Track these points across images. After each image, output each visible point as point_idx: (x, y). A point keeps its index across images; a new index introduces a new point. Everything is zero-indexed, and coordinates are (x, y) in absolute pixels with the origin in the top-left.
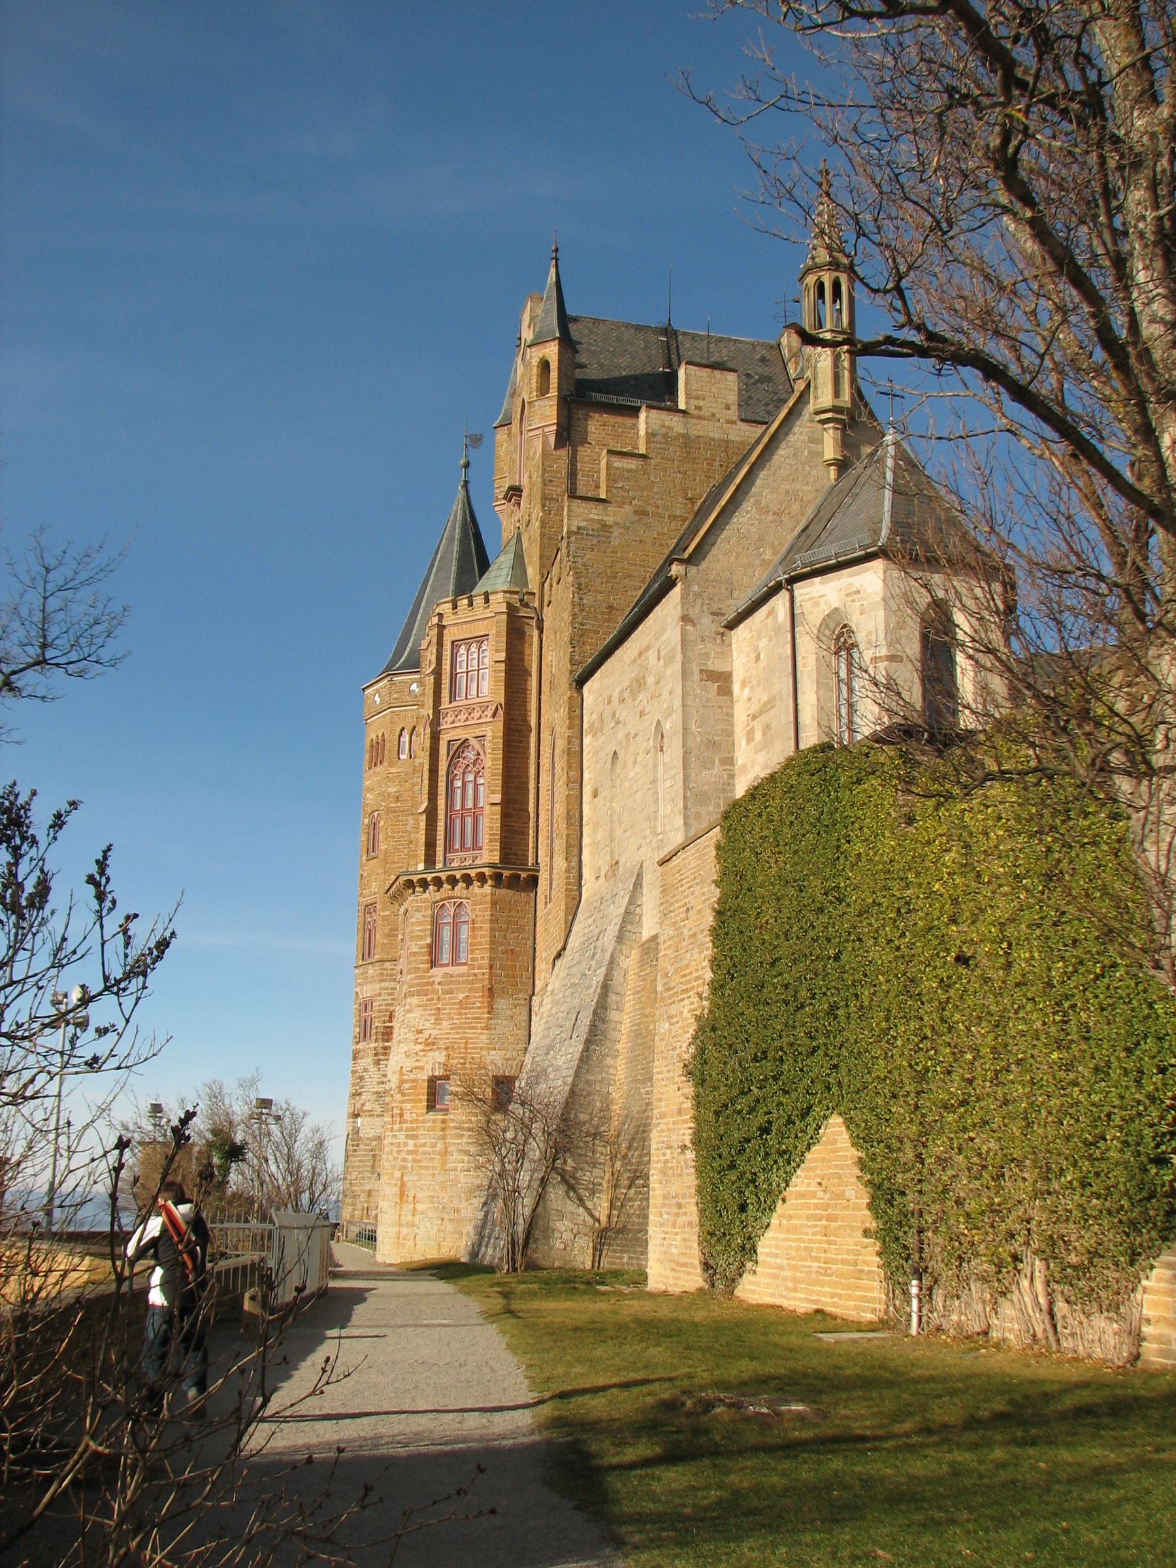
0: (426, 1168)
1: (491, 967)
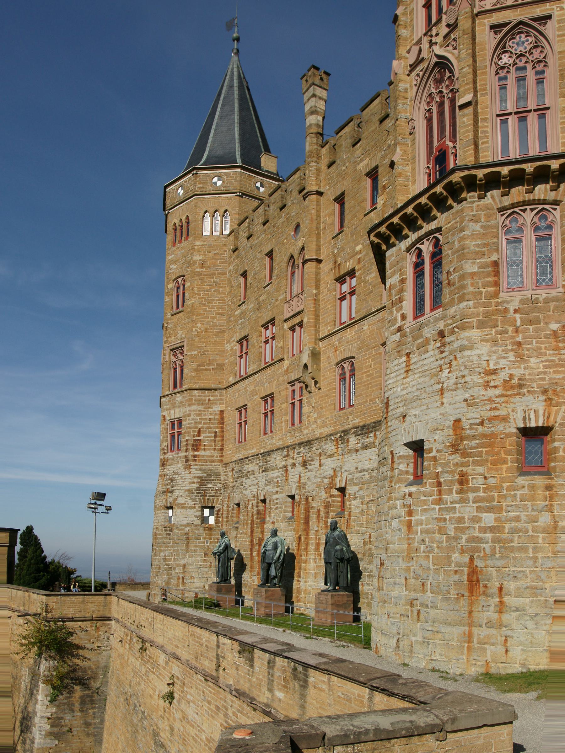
0: (524, 549)
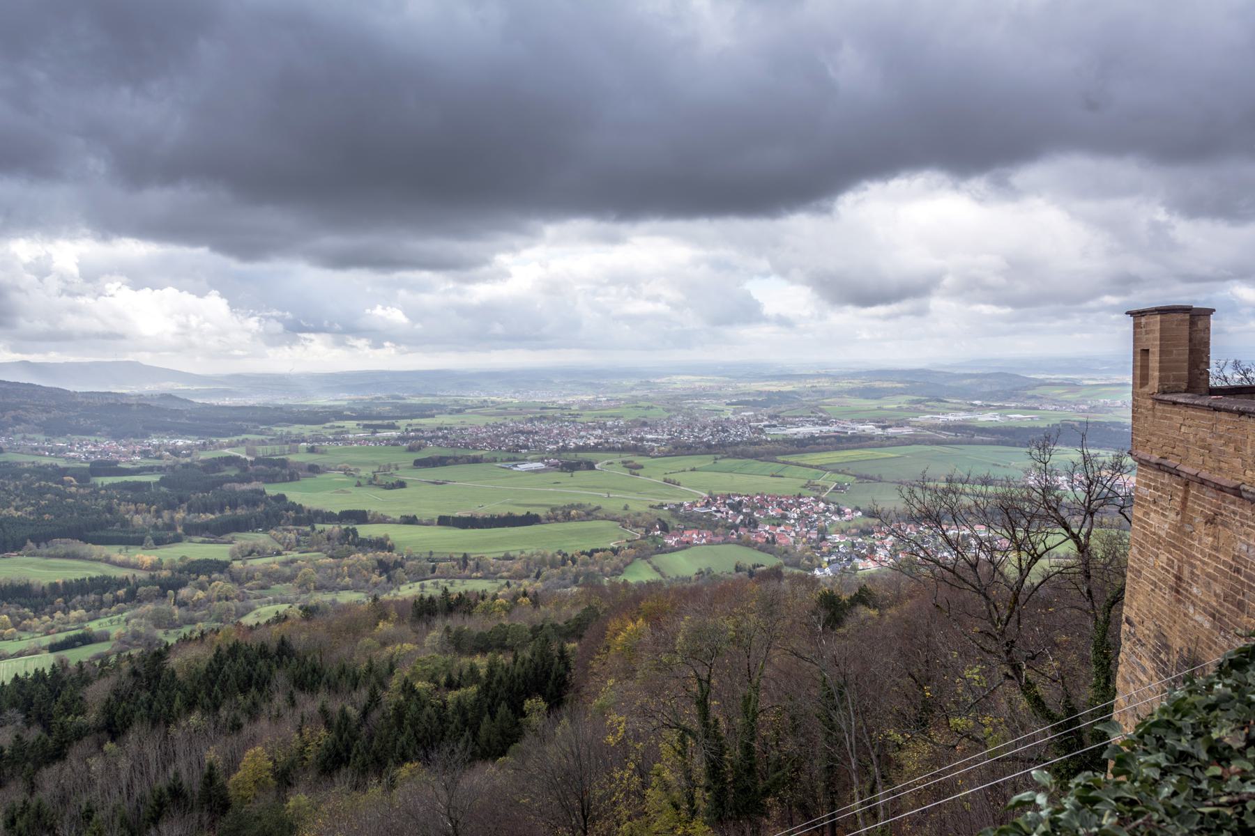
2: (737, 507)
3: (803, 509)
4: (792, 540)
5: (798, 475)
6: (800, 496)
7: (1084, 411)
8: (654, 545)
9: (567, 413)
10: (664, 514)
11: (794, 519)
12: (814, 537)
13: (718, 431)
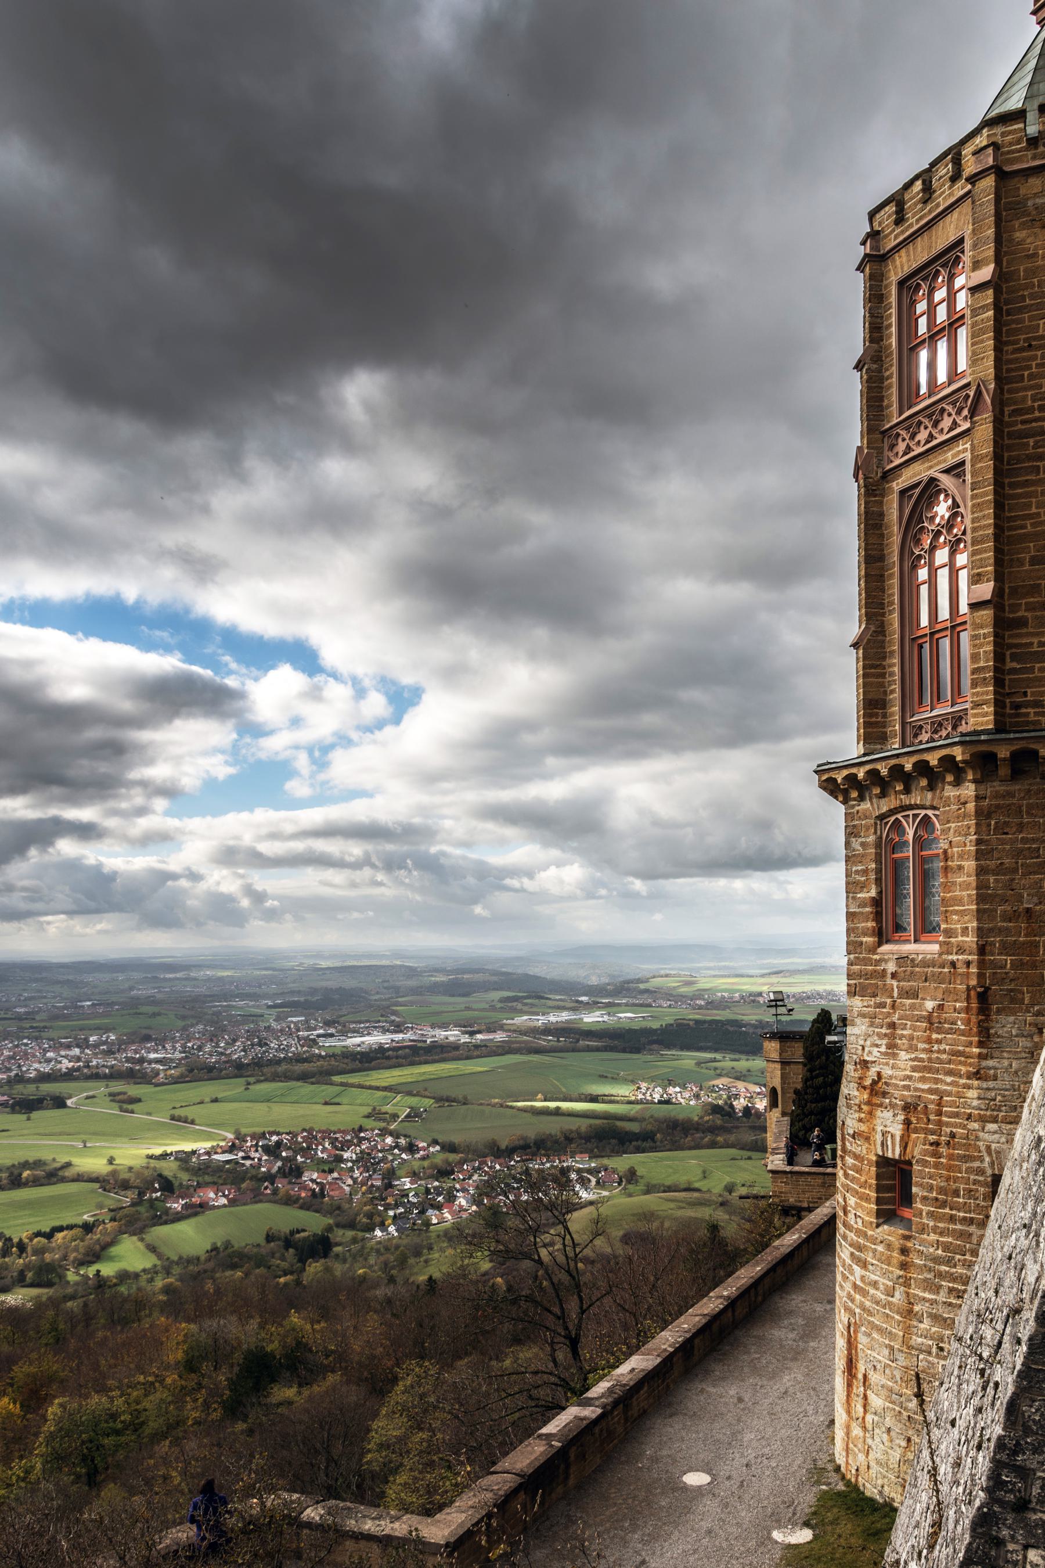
1: (982, 950)
2: (272, 1152)
3: (363, 1147)
4: (347, 1189)
5: (359, 1101)
6: (361, 1129)
7: (700, 1007)
8: (152, 1212)
9: (28, 1025)
10: (169, 1168)
11: (352, 1161)
12: (378, 1183)
13: (253, 1045)
